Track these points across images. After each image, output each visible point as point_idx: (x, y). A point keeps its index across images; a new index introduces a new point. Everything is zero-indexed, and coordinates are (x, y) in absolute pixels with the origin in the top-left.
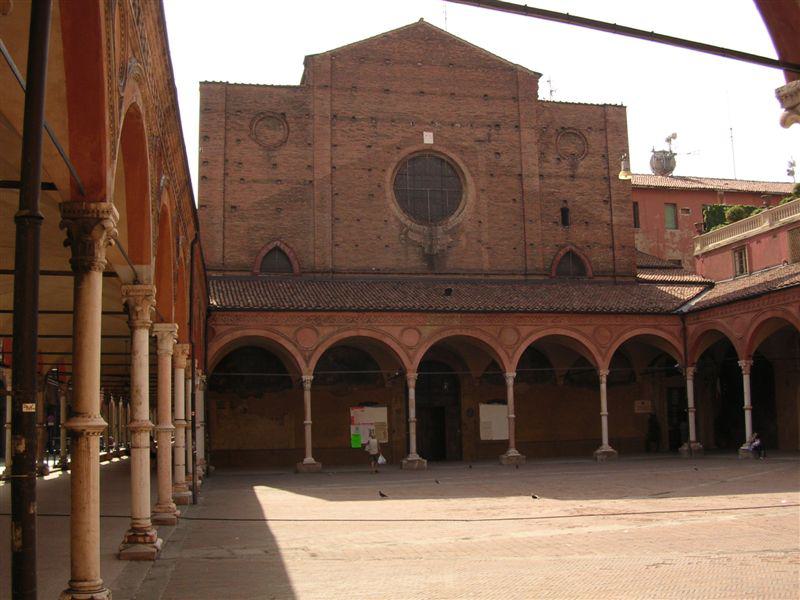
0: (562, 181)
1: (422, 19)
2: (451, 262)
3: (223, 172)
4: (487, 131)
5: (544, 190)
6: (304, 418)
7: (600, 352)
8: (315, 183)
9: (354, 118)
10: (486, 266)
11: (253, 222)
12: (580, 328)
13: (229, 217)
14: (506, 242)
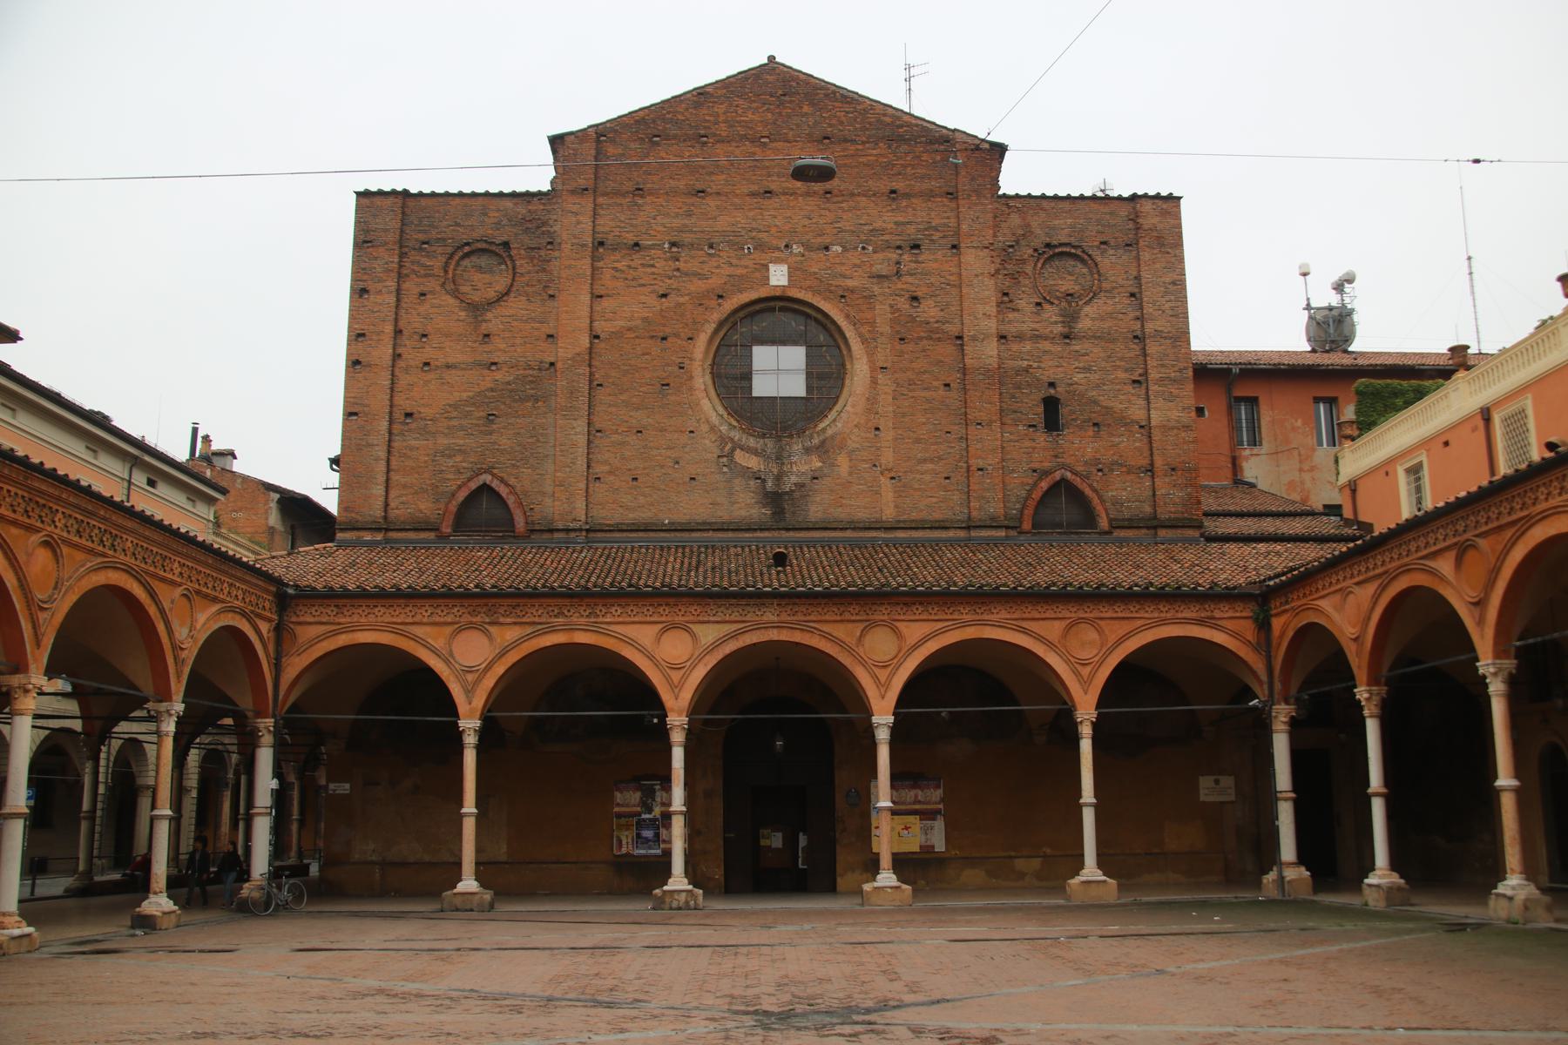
0: (1046, 345)
1: (771, 59)
4: (894, 256)
5: (1010, 363)
6: (459, 800)
7: (1077, 674)
8: (559, 365)
9: (637, 244)
10: (889, 514)
11: (443, 441)
14: (931, 466)
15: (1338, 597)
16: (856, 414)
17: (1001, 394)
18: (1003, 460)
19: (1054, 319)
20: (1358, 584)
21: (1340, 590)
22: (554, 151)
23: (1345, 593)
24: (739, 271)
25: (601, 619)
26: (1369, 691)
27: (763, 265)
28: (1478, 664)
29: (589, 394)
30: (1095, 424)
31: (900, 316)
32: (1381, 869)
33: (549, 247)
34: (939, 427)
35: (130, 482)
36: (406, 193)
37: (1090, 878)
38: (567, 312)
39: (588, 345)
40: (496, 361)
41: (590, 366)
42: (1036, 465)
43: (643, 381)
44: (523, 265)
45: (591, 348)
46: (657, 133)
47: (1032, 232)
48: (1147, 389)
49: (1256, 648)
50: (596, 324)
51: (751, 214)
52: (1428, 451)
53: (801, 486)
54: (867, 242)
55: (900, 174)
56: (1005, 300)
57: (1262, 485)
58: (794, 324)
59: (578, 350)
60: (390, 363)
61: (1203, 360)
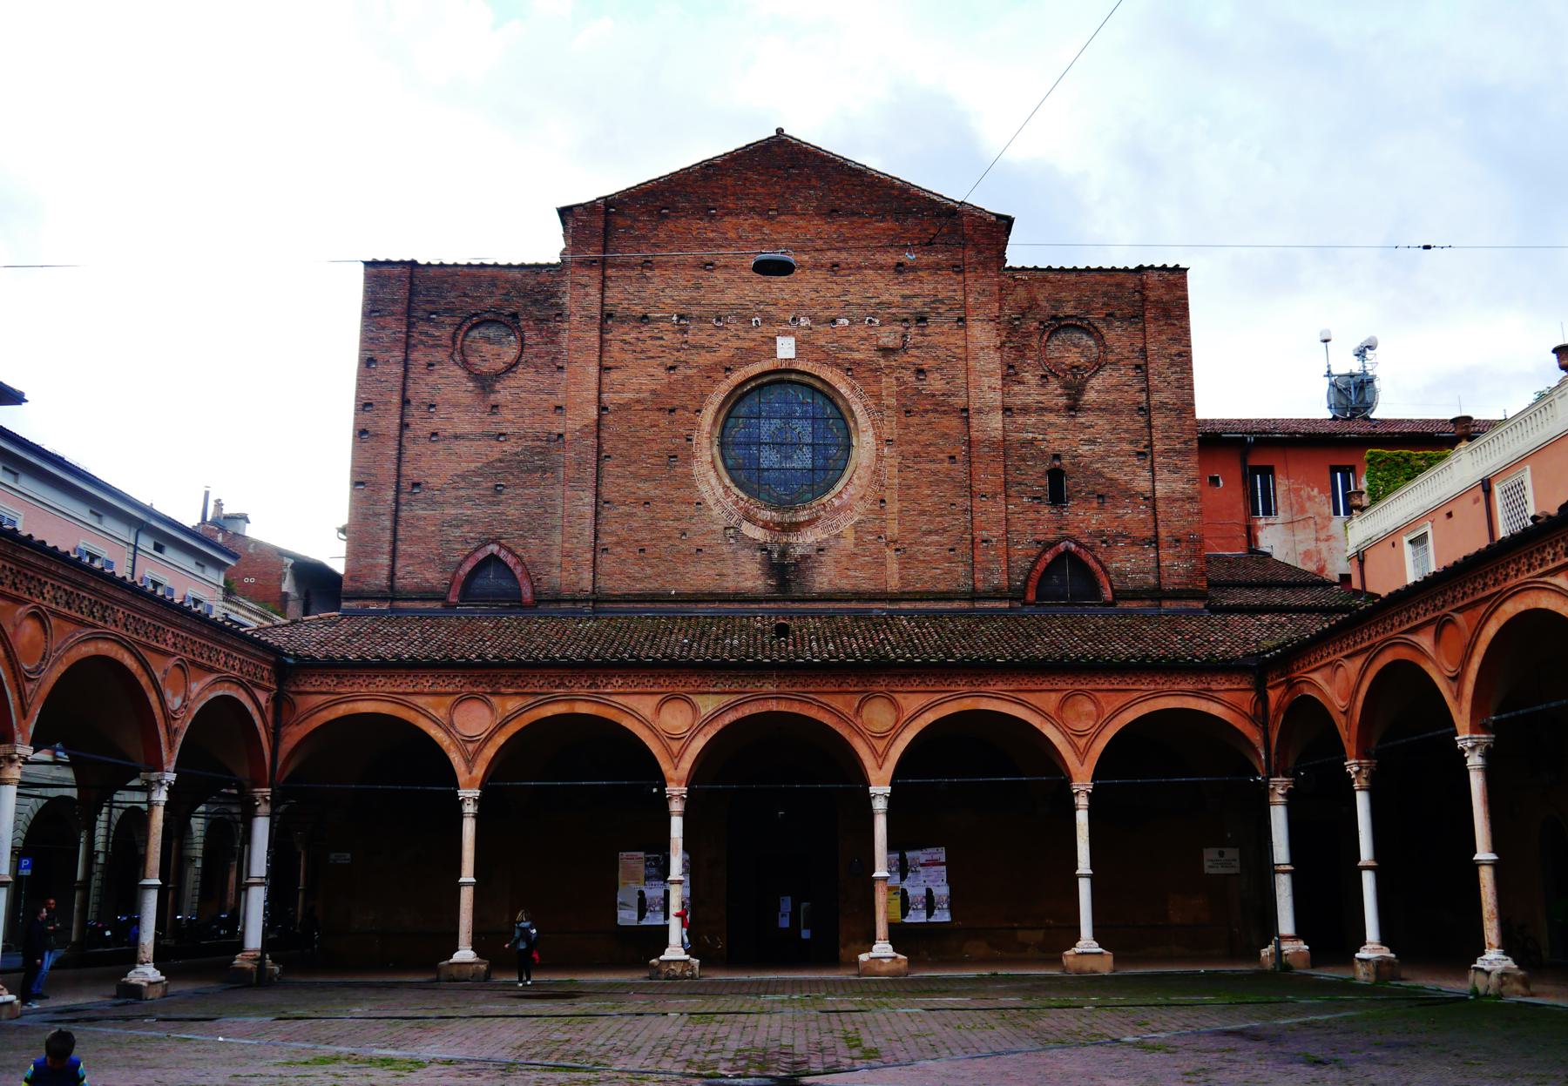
0: (1051, 418)
1: (780, 131)
8: (567, 437)
9: (645, 317)
10: (894, 584)
12: (1032, 698)
13: (409, 503)
14: (936, 538)
15: (1328, 671)
17: (1005, 466)
18: (1007, 532)
20: (1346, 657)
21: (1330, 663)
22: (564, 223)
23: (1336, 666)
24: (746, 344)
25: (601, 690)
26: (1358, 764)
27: (770, 338)
28: (1457, 738)
29: (598, 466)
30: (1099, 496)
31: (906, 388)
32: (1372, 943)
33: (558, 319)
35: (136, 547)
36: (413, 264)
37: (1085, 950)
38: (575, 384)
39: (596, 417)
40: (504, 431)
41: (598, 437)
42: (1041, 537)
43: (651, 453)
44: (531, 336)
45: (599, 420)
46: (662, 204)
47: (1039, 306)
48: (1152, 461)
49: (1253, 720)
50: (604, 396)
51: (759, 287)
52: (1432, 522)
53: (805, 558)
54: (874, 315)
56: (1011, 374)
57: (1277, 556)
58: (800, 396)
60: (397, 433)
61: (1208, 429)
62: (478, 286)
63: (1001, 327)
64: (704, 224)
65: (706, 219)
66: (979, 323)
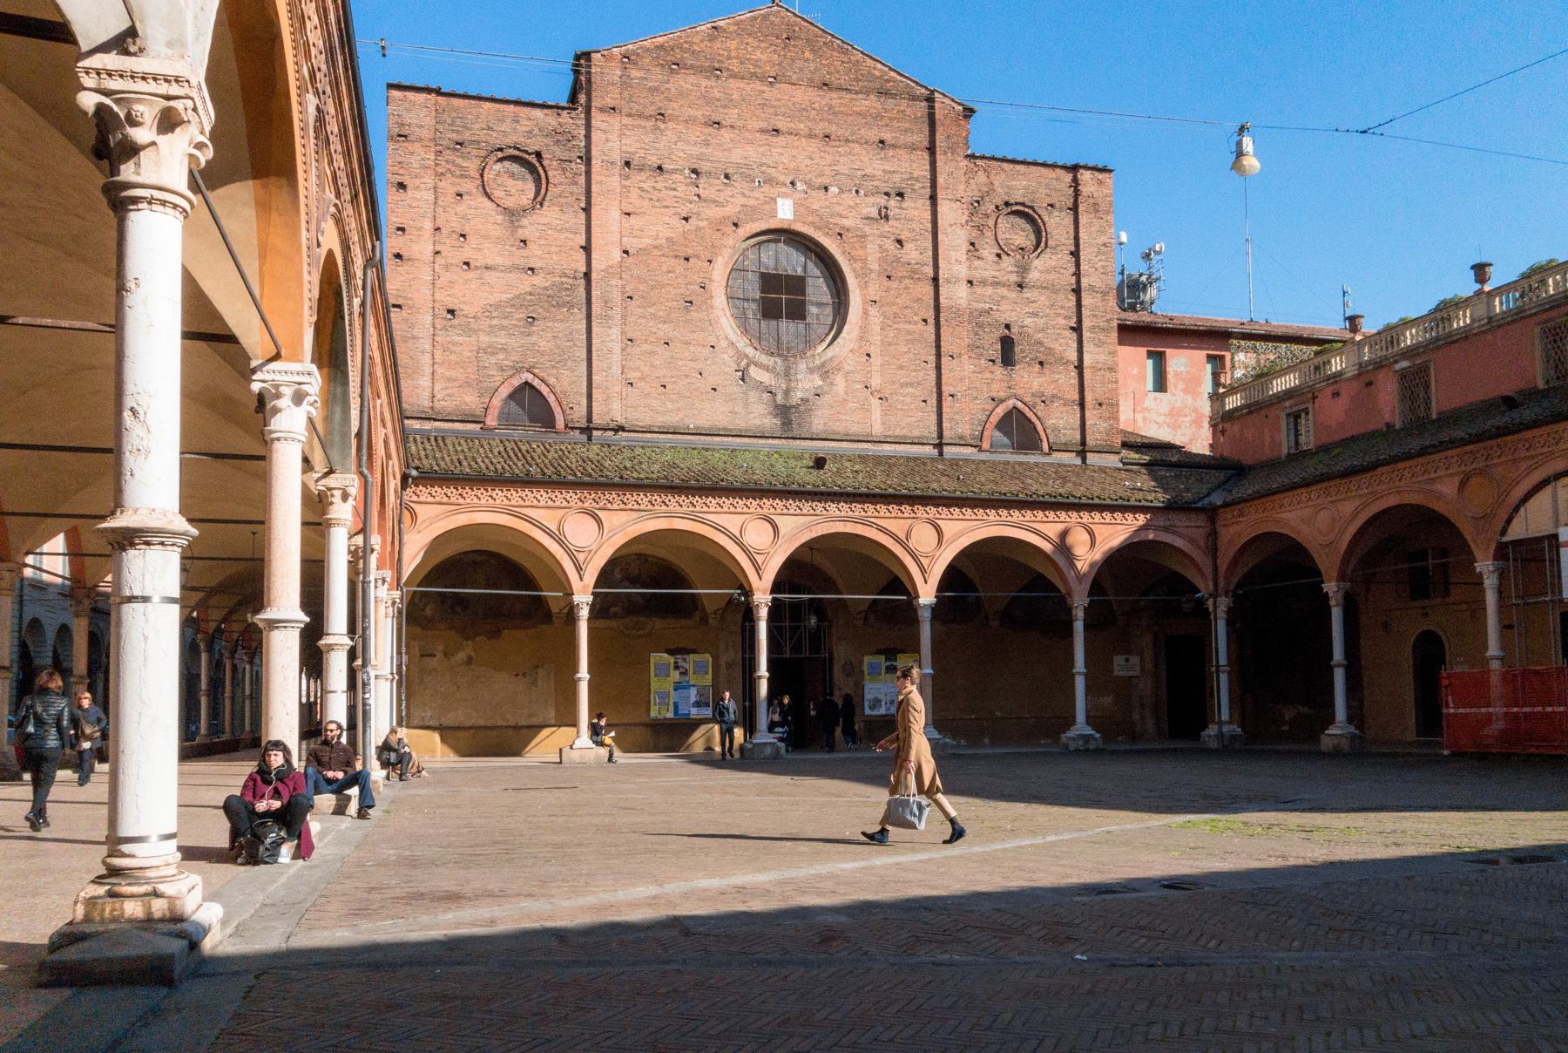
0: (1003, 291)
2: (819, 421)
3: (431, 247)
4: (882, 200)
6: (575, 669)
10: (878, 430)
11: (485, 339)
14: (911, 390)
16: (851, 340)
19: (1010, 269)
24: (752, 202)
34: (918, 357)
42: (994, 394)
46: (676, 61)
50: (625, 239)
51: (761, 149)
55: (887, 126)
59: (611, 263)
60: (432, 259)
62: (502, 120)
63: (965, 206)
64: (712, 82)
65: (713, 79)
66: (948, 202)
